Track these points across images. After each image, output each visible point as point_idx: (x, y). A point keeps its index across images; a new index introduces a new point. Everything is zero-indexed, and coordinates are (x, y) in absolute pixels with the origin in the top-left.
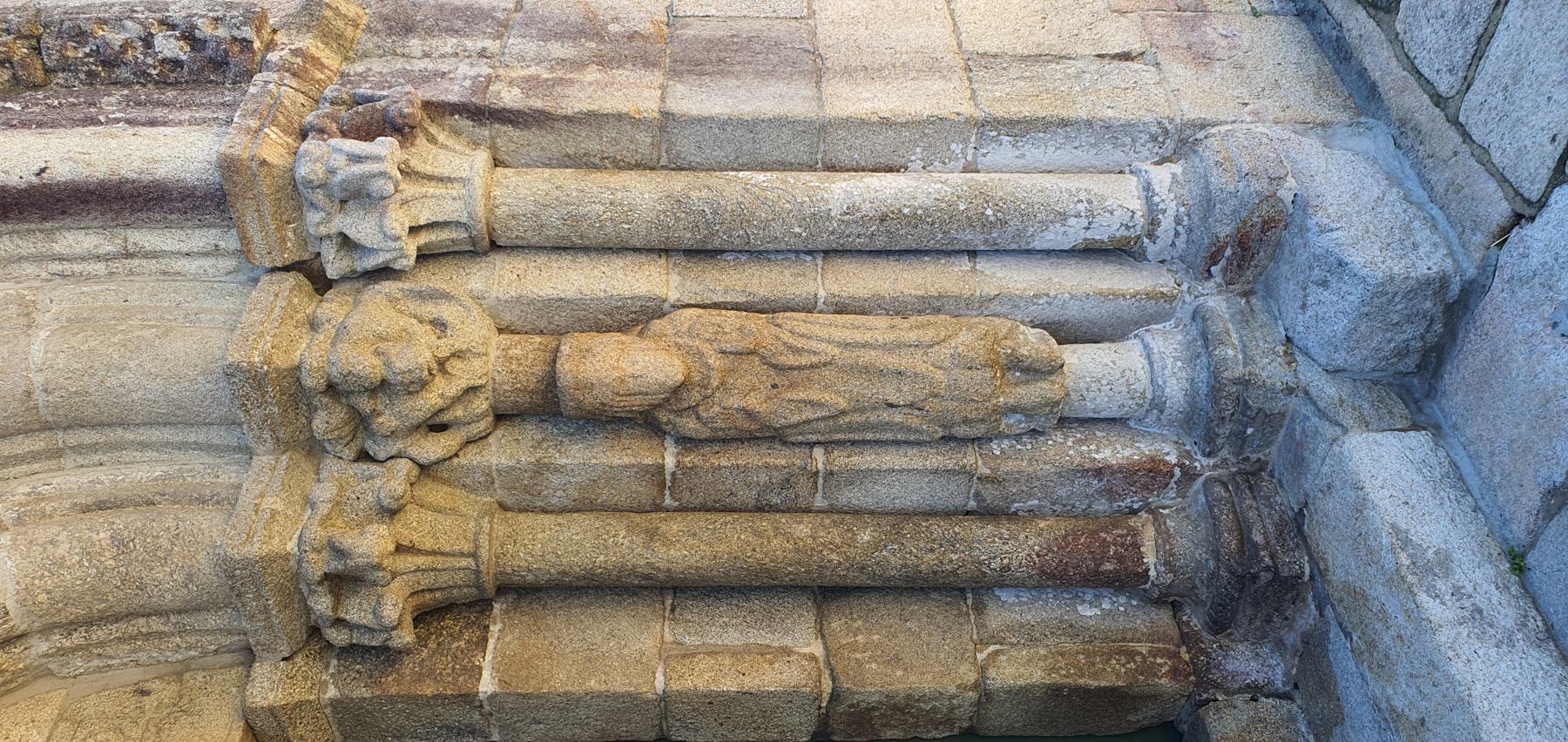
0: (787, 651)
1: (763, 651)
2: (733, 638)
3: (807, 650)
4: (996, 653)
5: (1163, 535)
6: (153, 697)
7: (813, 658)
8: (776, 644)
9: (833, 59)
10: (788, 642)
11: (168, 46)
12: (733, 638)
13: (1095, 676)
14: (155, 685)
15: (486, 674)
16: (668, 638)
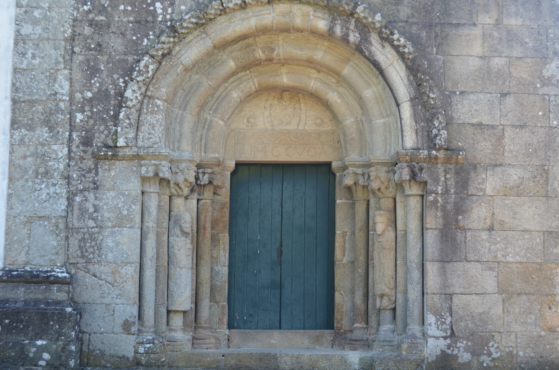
0: (344, 255)
1: (344, 251)
2: (347, 246)
3: (344, 259)
4: (342, 295)
5: (359, 329)
6: (337, 144)
7: (342, 260)
8: (346, 253)
9: (449, 266)
10: (346, 255)
11: (434, 131)
12: (347, 246)
13: (337, 311)
14: (340, 143)
15: (341, 201)
16: (347, 233)
